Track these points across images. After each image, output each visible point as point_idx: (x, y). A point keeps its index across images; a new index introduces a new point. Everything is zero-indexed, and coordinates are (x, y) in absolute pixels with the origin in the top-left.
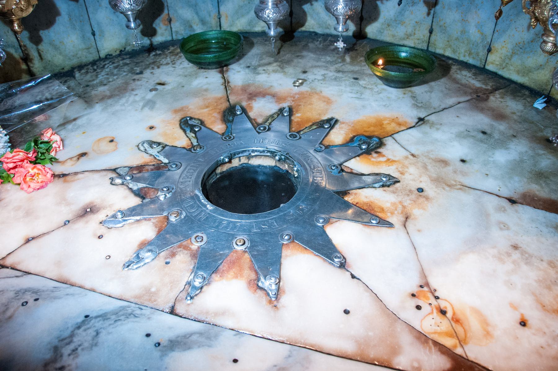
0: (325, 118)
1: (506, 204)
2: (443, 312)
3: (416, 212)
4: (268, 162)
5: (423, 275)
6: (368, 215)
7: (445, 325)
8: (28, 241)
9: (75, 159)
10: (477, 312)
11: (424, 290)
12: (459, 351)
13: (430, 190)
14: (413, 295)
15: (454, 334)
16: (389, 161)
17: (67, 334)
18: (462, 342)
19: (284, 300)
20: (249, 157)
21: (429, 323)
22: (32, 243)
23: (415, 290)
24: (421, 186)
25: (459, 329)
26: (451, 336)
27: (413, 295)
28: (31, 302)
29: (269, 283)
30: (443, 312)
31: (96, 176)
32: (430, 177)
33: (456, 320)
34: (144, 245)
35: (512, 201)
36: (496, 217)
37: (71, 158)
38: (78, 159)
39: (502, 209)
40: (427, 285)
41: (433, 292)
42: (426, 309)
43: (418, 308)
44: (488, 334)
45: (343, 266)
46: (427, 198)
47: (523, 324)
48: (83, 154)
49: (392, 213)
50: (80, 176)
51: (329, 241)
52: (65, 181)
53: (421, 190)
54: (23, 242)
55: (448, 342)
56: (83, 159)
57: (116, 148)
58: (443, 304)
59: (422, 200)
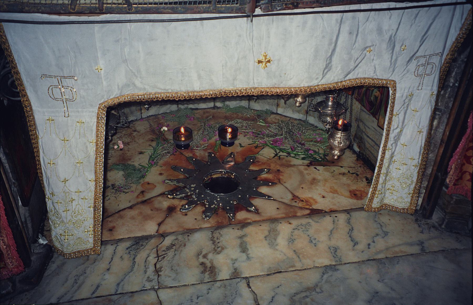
0: (229, 153)
1: (306, 167)
2: (303, 201)
3: (281, 177)
4: (220, 175)
6: (266, 183)
8: (159, 225)
9: (141, 194)
10: (310, 198)
11: (295, 197)
12: (311, 208)
13: (281, 169)
14: (293, 199)
15: (308, 205)
16: (264, 164)
17: (211, 236)
18: (311, 206)
19: (259, 211)
20: (211, 175)
21: (300, 205)
22: (161, 225)
23: (292, 198)
24: (278, 169)
25: (308, 203)
26: (306, 205)
27: (293, 199)
30: (303, 201)
31: (159, 198)
32: (279, 165)
33: (307, 201)
34: (204, 212)
35: (308, 166)
36: (305, 172)
37: (139, 195)
38: (143, 194)
39: (307, 169)
40: (295, 196)
41: (297, 197)
43: (296, 202)
44: (316, 202)
46: (282, 172)
47: (324, 197)
48: (143, 192)
49: (274, 180)
50: (152, 200)
51: (261, 193)
52: (148, 203)
53: (279, 170)
54: (158, 226)
55: (307, 207)
56: (144, 193)
57: (155, 186)
58: (302, 199)
59: (280, 173)
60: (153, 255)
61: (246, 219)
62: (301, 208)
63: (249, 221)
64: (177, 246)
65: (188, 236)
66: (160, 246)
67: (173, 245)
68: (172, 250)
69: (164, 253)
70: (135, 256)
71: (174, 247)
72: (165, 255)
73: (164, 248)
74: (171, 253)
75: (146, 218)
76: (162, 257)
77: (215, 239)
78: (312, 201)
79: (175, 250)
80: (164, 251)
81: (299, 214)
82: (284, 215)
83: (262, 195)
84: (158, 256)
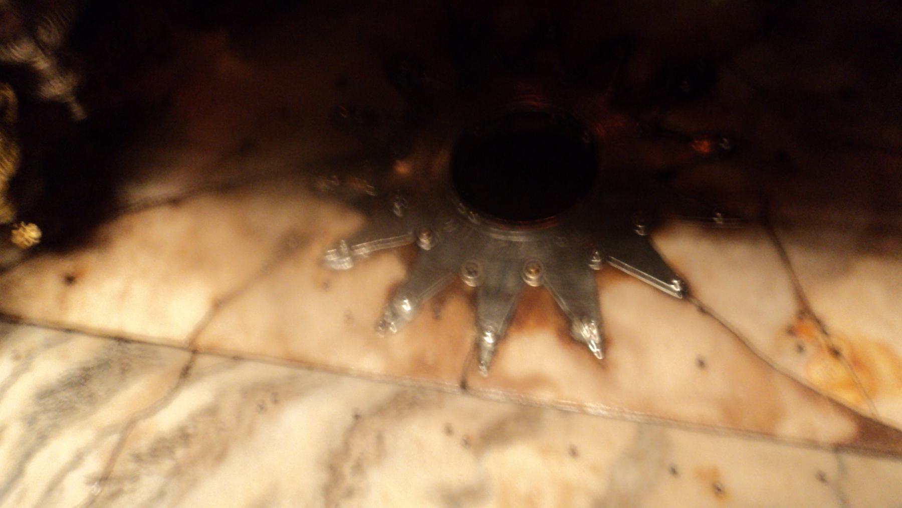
2: (836, 353)
5: (801, 298)
7: (839, 371)
8: (218, 305)
10: (886, 350)
12: (865, 409)
14: (791, 331)
15: (853, 384)
21: (818, 371)
28: (269, 404)
29: (588, 332)
30: (836, 353)
33: (858, 363)
34: (395, 293)
42: (810, 348)
45: (687, 293)
55: (848, 397)
58: (835, 342)
60: (93, 465)
61: (537, 381)
62: (810, 393)
63: (544, 396)
64: (195, 448)
65: (262, 408)
66: (143, 425)
67: (183, 436)
68: (167, 464)
69: (132, 466)
70: (42, 439)
71: (180, 453)
72: (127, 486)
73: (143, 444)
74: (151, 481)
75: (195, 260)
76: (113, 488)
77: (347, 469)
78: (884, 368)
79: (177, 472)
80: (138, 458)
81: (790, 427)
82: (711, 413)
83: (662, 271)
84: (104, 479)
